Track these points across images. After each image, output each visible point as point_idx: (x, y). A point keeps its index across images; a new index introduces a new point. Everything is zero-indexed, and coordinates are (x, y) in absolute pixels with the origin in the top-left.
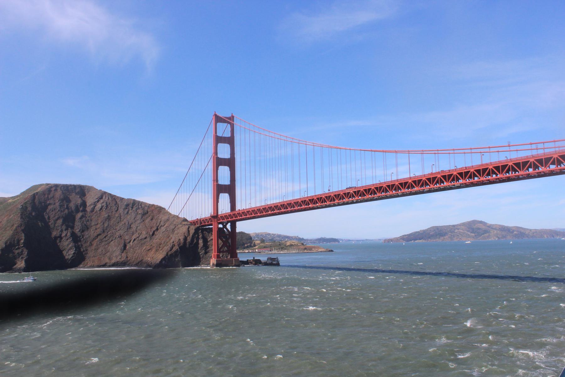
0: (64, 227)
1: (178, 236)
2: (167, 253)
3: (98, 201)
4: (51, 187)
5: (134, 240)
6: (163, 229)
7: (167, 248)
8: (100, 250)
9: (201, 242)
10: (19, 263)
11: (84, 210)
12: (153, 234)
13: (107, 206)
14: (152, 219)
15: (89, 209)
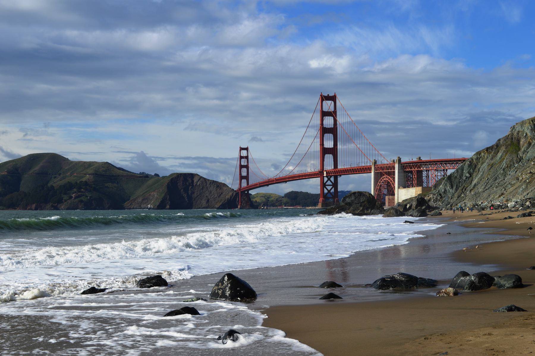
0: (184, 193)
1: (228, 197)
2: (222, 204)
3: (199, 181)
4: (179, 175)
5: (212, 198)
6: (224, 193)
7: (223, 201)
8: (198, 202)
9: (237, 199)
10: (167, 206)
11: (193, 185)
12: (220, 195)
13: (202, 183)
14: (220, 189)
15: (194, 185)
